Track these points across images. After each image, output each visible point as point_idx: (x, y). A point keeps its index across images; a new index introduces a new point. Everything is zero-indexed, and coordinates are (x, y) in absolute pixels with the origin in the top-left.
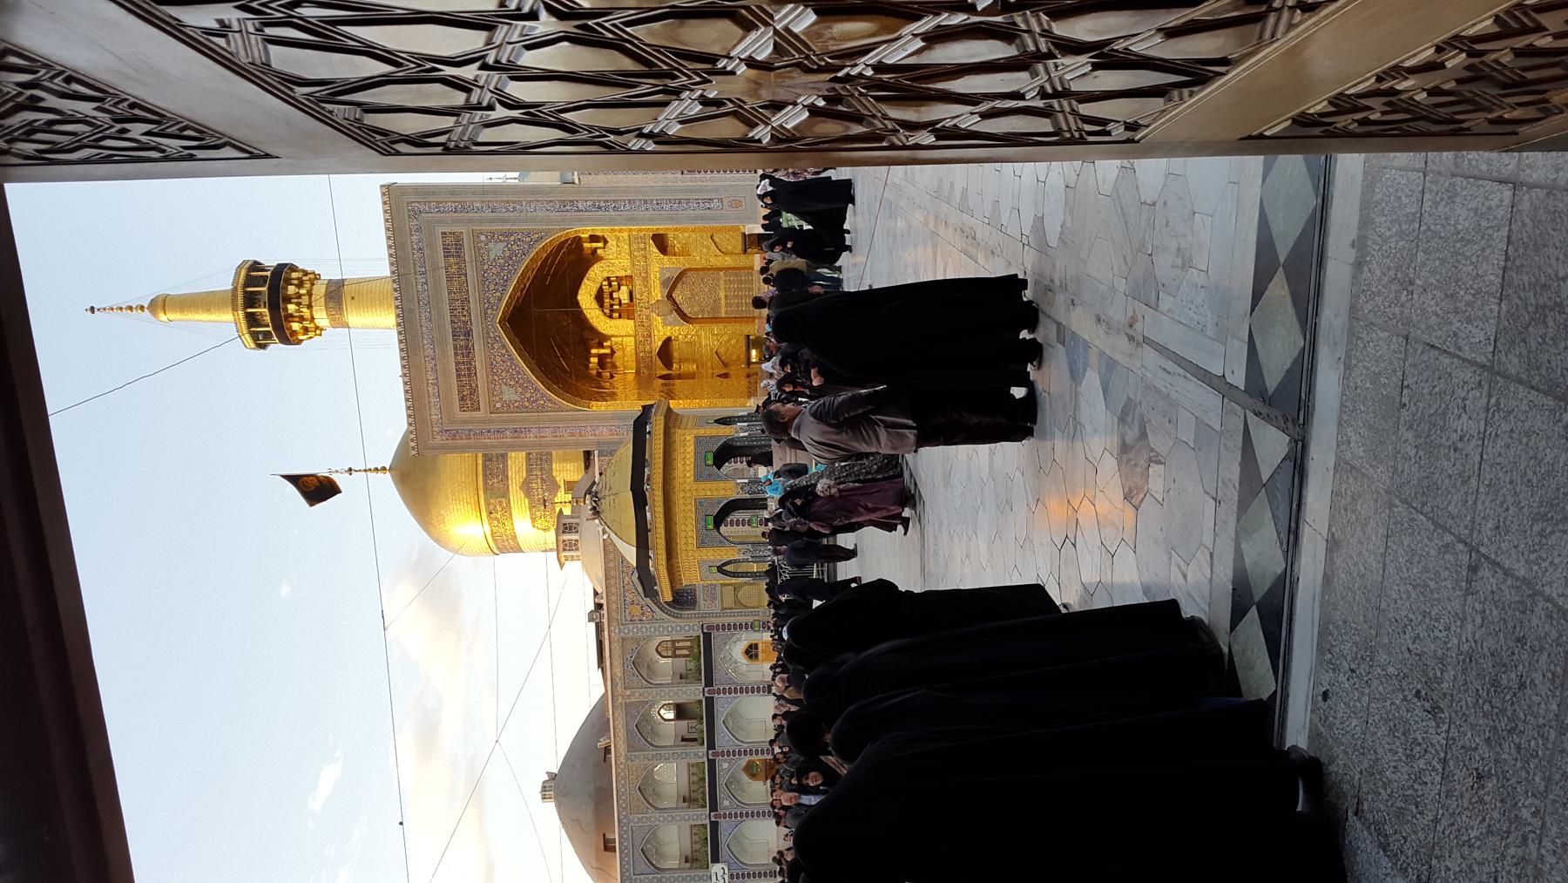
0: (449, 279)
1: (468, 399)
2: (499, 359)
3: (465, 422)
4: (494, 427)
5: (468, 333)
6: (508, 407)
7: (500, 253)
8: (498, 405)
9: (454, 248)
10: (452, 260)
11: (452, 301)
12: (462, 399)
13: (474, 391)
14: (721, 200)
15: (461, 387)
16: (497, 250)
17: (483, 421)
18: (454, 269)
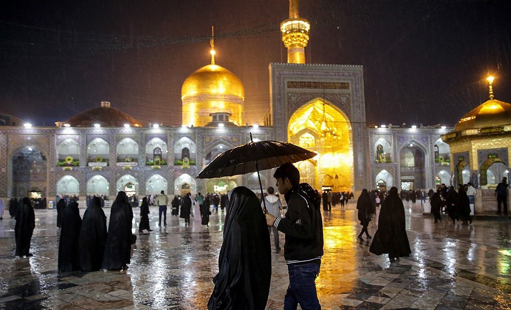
0: (334, 83)
1: (292, 85)
2: (306, 96)
3: (284, 82)
4: (282, 92)
5: (315, 87)
6: (289, 98)
7: (343, 100)
8: (290, 95)
9: (344, 86)
10: (340, 85)
11: (326, 83)
12: (292, 82)
13: (295, 87)
14: (362, 177)
15: (296, 82)
16: (344, 100)
17: (284, 89)
18: (337, 85)
